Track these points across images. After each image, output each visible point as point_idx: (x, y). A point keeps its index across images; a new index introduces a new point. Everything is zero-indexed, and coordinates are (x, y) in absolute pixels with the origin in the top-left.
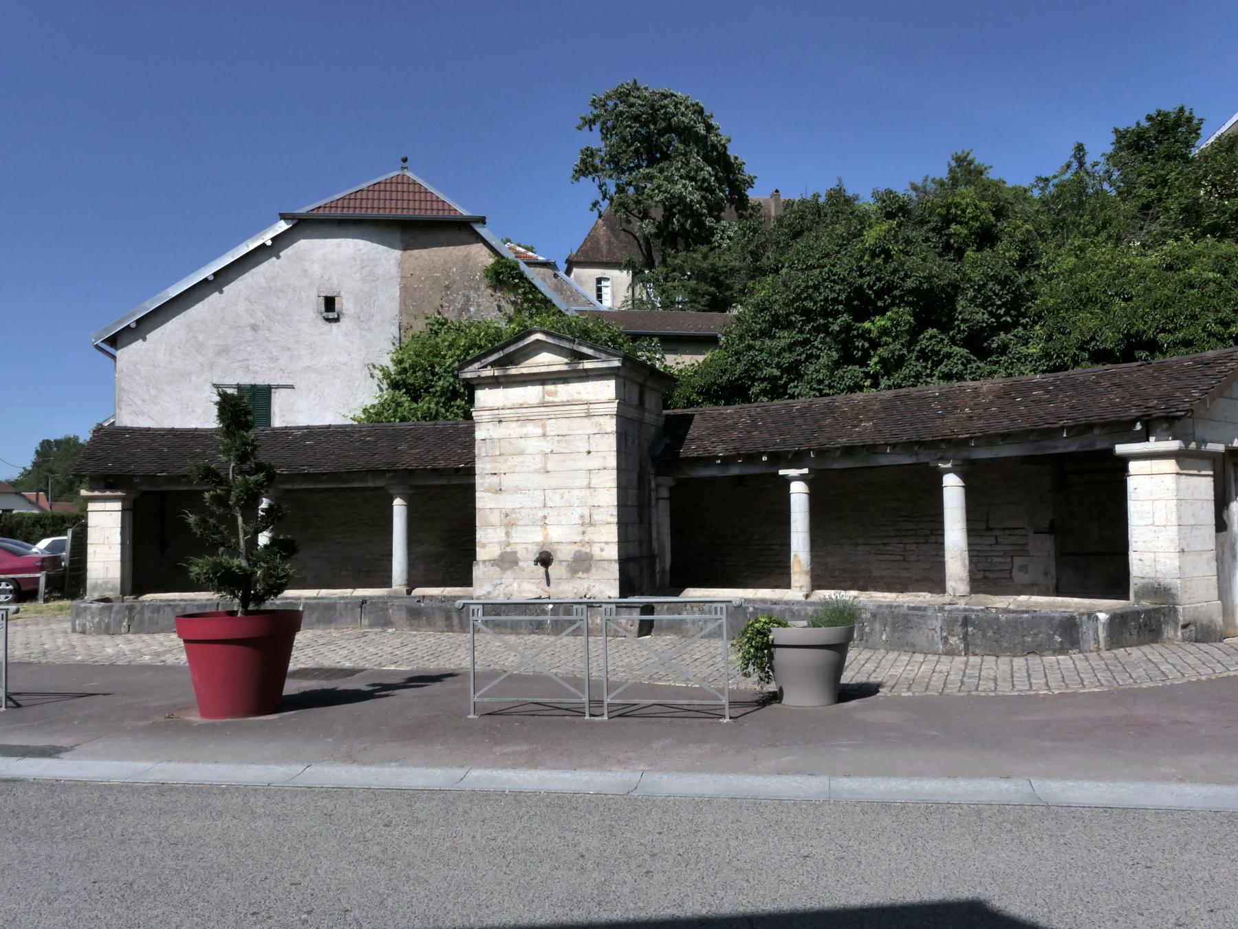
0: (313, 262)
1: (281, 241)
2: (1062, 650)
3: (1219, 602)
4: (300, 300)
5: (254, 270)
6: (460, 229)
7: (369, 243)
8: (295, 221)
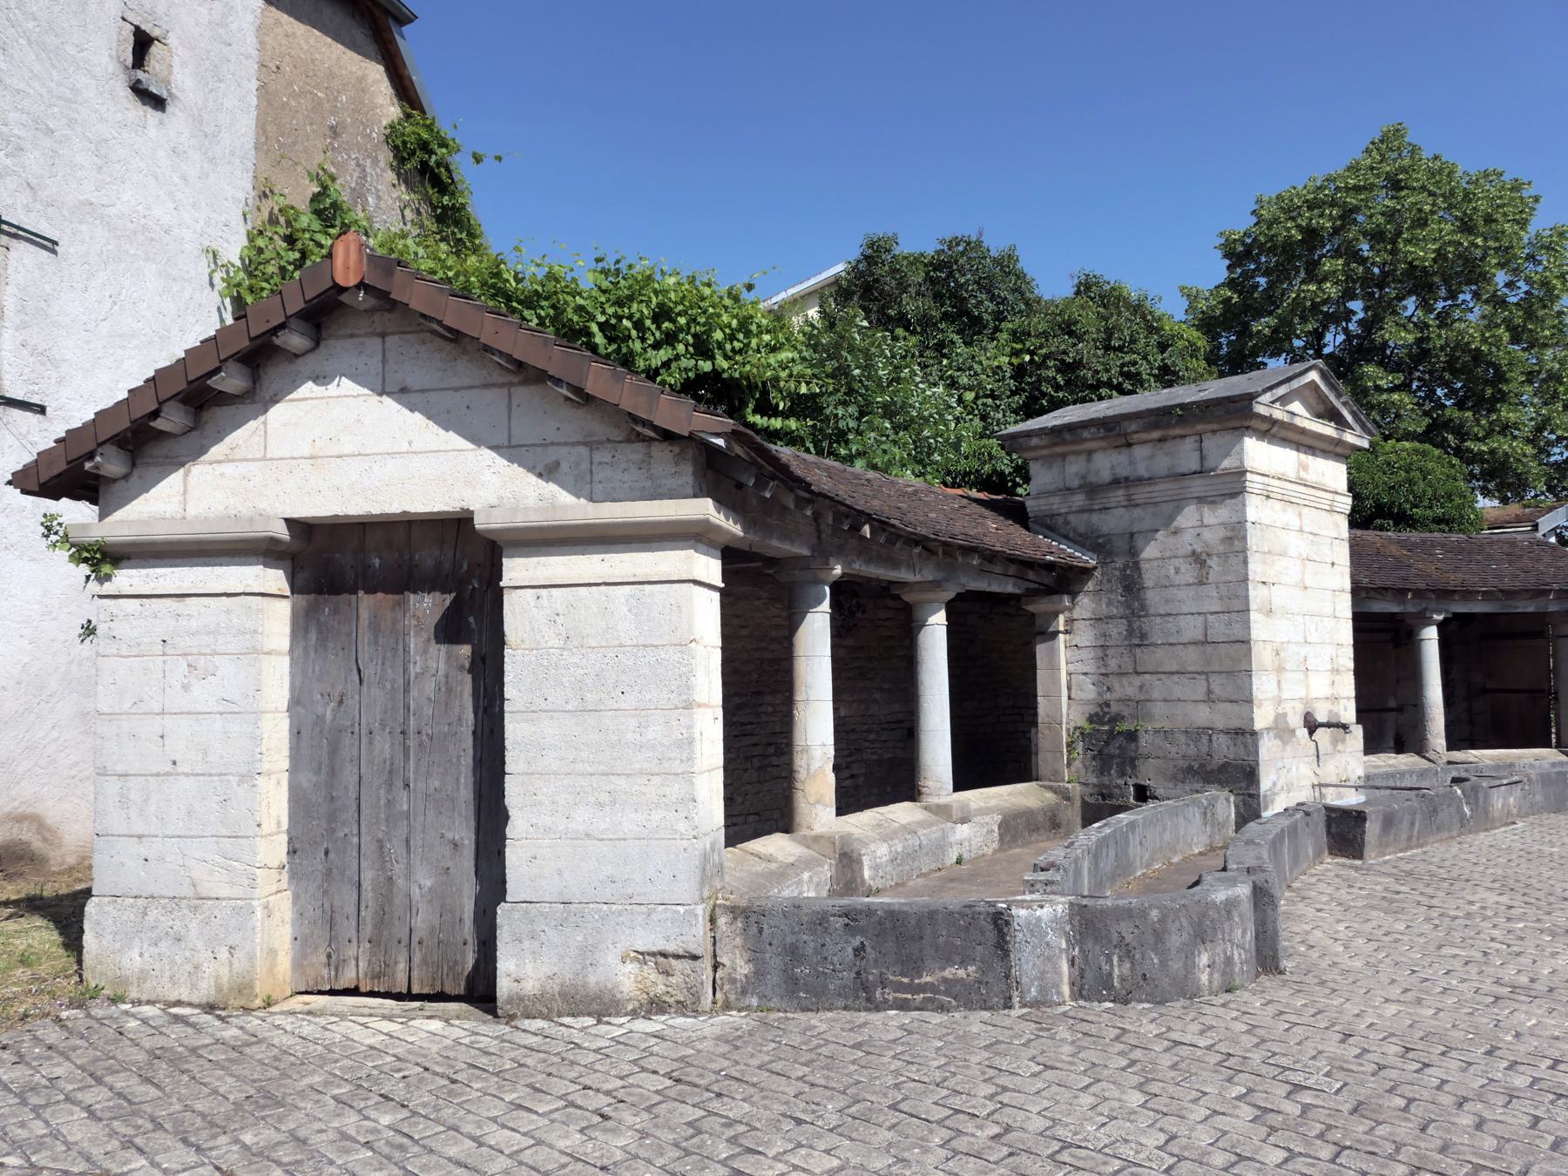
6: (353, 17)
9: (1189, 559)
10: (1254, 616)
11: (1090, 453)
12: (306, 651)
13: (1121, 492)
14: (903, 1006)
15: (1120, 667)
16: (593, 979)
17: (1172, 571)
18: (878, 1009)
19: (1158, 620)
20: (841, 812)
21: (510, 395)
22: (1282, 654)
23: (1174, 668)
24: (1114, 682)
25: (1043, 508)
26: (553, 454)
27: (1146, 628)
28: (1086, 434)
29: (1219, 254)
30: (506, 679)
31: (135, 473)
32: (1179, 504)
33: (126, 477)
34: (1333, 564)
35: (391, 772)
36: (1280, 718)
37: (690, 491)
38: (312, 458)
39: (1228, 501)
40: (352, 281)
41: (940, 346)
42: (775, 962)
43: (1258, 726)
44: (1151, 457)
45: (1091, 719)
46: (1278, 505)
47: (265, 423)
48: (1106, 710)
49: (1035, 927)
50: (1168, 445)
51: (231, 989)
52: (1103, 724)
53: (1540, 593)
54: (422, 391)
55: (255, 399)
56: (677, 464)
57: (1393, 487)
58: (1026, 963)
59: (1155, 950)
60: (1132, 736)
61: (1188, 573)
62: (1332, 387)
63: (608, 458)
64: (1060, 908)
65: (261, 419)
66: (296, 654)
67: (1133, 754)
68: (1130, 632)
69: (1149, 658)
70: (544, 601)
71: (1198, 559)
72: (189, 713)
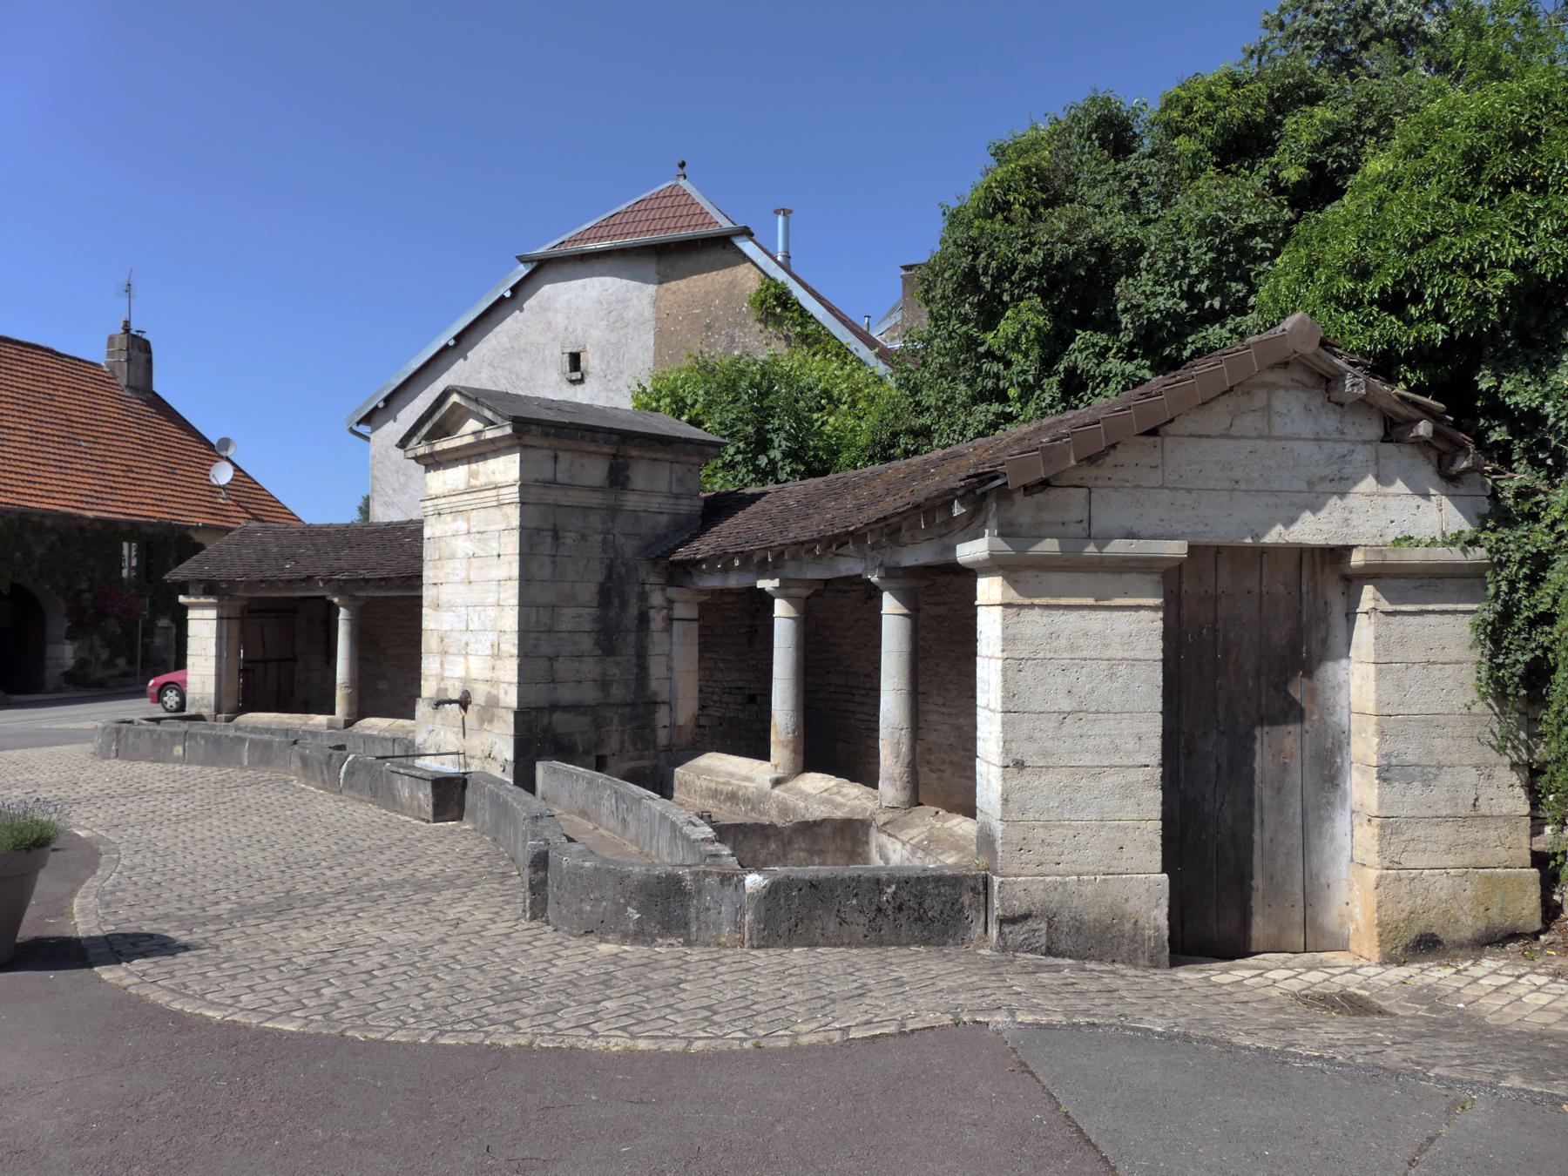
0: (557, 311)
1: (520, 290)
2: (640, 936)
3: (1165, 875)
4: (544, 361)
5: (497, 329)
7: (617, 280)
8: (535, 264)
22: (446, 640)
46: (449, 518)
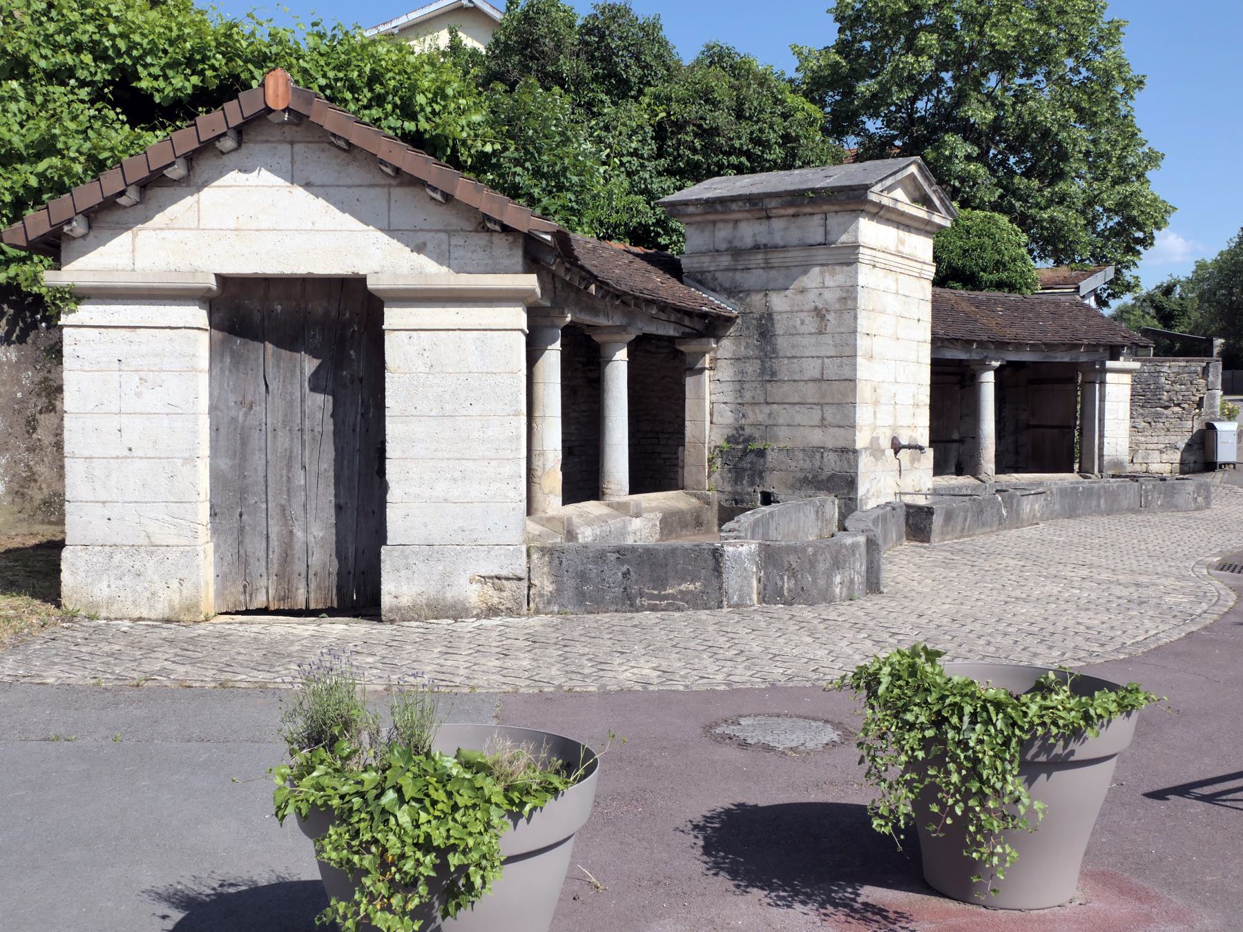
9: (812, 313)
10: (859, 360)
11: (736, 222)
12: (222, 370)
13: (760, 256)
14: (654, 609)
15: (754, 398)
16: (450, 595)
17: (799, 322)
18: (637, 611)
19: (786, 361)
20: (566, 501)
21: (389, 193)
22: (878, 391)
23: (797, 400)
24: (748, 410)
25: (696, 265)
26: (421, 237)
27: (776, 367)
28: (734, 206)
29: (832, 17)
30: (386, 394)
31: (92, 234)
32: (805, 268)
33: (84, 236)
34: (919, 320)
35: (290, 457)
36: (875, 440)
37: (520, 267)
38: (236, 230)
39: (845, 268)
40: (281, 107)
41: (589, 105)
42: (570, 583)
43: (858, 446)
44: (786, 229)
45: (728, 440)
46: (881, 273)
47: (198, 202)
48: (741, 432)
49: (738, 558)
50: (800, 220)
51: (181, 608)
52: (738, 443)
53: (1074, 346)
54: (323, 186)
55: (190, 183)
56: (511, 249)
57: (968, 250)
58: (732, 580)
59: (809, 572)
60: (761, 453)
61: (811, 325)
62: (926, 178)
63: (461, 242)
64: (753, 546)
65: (196, 196)
66: (214, 373)
67: (761, 468)
68: (763, 371)
69: (777, 391)
70: (414, 340)
71: (819, 314)
72: (142, 414)
